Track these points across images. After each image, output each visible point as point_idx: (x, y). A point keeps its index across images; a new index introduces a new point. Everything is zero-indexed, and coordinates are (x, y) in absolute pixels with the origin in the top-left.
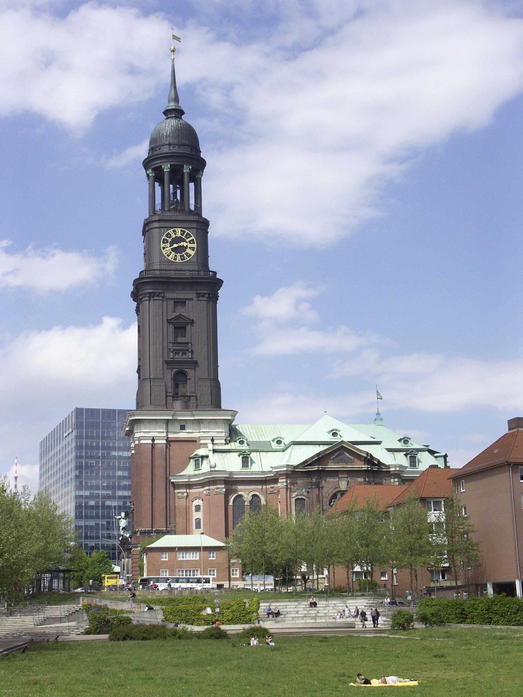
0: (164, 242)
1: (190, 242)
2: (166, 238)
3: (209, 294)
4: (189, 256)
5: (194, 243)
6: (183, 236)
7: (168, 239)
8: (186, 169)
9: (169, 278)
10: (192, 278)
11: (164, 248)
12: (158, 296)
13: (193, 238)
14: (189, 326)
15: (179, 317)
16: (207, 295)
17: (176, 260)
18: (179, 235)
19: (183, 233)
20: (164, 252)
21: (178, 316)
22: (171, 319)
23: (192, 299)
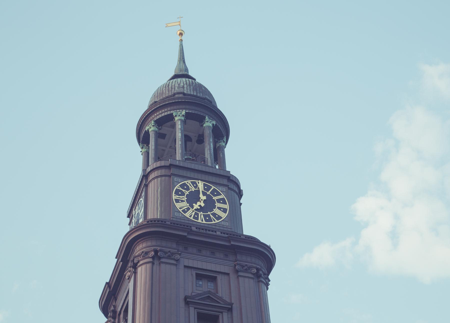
2: (181, 189)
4: (219, 218)
5: (226, 204)
6: (208, 191)
7: (183, 190)
9: (191, 232)
12: (169, 257)
14: (225, 315)
16: (255, 271)
17: (198, 220)
20: (178, 205)
23: (228, 274)
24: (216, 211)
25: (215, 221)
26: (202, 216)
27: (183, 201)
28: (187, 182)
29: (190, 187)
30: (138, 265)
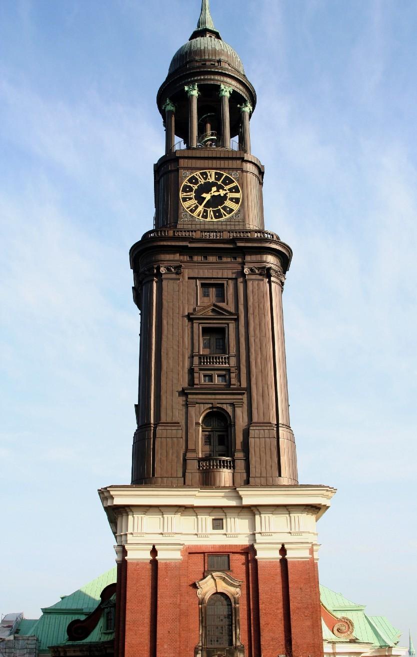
4: (231, 210)
6: (219, 181)
7: (191, 185)
10: (233, 241)
18: (212, 179)
19: (218, 176)
20: (186, 205)
25: (225, 216)
26: (212, 213)
27: (190, 199)
28: (196, 175)
29: (199, 179)
30: (143, 282)
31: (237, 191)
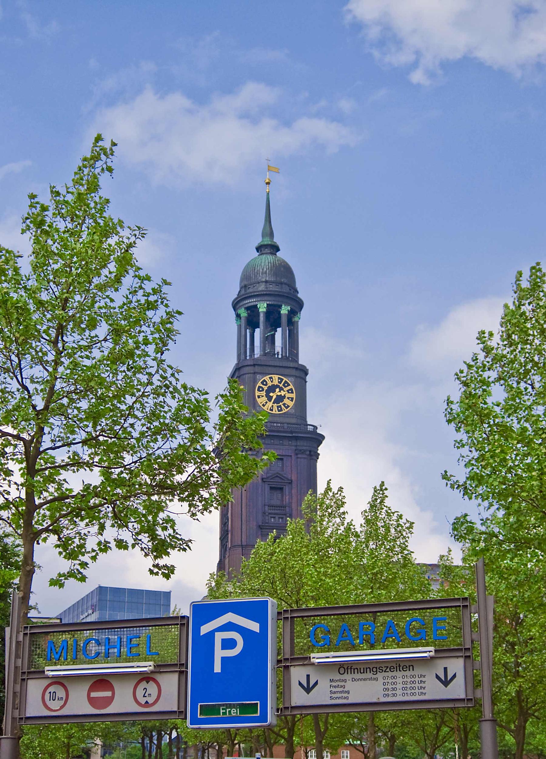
0: (259, 390)
1: (288, 391)
2: (262, 385)
3: (310, 451)
4: (288, 406)
8: (285, 310)
10: (292, 432)
11: (259, 397)
13: (291, 387)
14: (287, 487)
15: (277, 476)
16: (308, 453)
18: (276, 382)
20: (259, 401)
21: (274, 474)
22: (267, 478)
24: (286, 401)
27: (262, 396)
31: (292, 392)
